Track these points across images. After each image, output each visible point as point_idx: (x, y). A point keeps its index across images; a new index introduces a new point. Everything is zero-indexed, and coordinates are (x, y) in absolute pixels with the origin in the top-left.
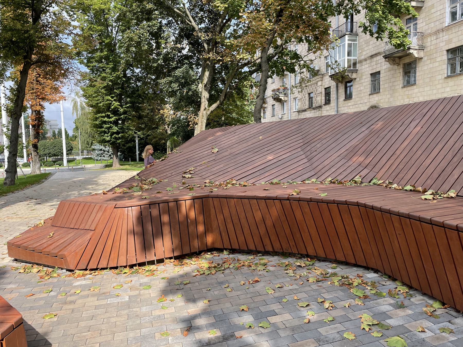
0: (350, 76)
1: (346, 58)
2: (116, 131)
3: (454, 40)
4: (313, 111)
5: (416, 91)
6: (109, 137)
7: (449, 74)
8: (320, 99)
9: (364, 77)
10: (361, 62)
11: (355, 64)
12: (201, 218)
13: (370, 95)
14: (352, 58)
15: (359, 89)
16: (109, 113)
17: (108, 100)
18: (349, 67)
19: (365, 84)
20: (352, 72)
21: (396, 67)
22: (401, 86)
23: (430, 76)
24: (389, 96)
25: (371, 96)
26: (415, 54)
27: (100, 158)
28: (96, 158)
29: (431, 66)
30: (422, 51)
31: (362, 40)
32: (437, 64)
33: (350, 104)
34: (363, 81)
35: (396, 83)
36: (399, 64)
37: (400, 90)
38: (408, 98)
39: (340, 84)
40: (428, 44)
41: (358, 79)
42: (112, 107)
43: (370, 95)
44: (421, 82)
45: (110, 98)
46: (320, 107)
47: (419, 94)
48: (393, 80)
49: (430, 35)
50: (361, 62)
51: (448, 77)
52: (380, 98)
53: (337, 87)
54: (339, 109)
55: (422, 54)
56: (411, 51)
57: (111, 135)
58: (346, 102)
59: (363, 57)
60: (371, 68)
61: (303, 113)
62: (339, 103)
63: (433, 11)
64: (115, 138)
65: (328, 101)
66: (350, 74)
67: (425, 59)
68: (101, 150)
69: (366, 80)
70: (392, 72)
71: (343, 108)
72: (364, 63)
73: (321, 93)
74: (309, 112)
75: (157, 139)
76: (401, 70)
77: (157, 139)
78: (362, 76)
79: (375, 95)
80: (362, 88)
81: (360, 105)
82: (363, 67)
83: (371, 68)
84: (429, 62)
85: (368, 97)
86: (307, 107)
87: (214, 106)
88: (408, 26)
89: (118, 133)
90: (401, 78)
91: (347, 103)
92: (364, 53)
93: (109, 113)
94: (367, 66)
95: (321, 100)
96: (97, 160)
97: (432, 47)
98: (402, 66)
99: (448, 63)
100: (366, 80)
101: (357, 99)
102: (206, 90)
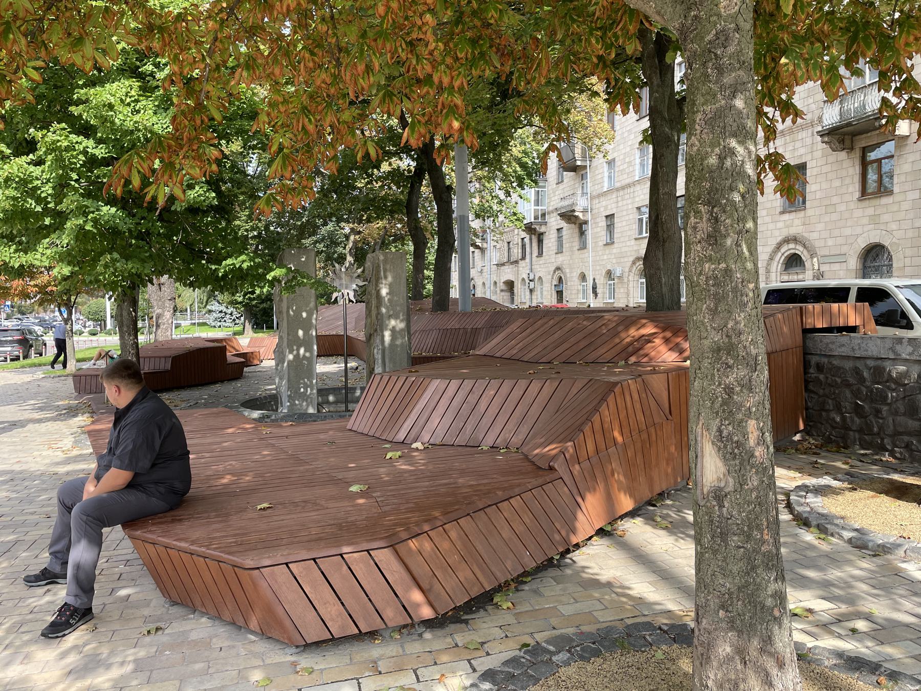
1: (533, 207)
3: (609, 207)
4: (511, 266)
6: (242, 297)
7: (608, 241)
8: (516, 252)
9: (552, 232)
10: (549, 213)
11: (543, 215)
14: (540, 208)
18: (536, 218)
20: (541, 224)
22: (577, 248)
24: (569, 258)
25: (557, 256)
26: (580, 215)
27: (219, 324)
28: (213, 324)
31: (550, 188)
32: (599, 229)
33: (541, 262)
36: (575, 224)
39: (533, 236)
41: (547, 234)
46: (516, 262)
50: (549, 213)
51: (607, 244)
52: (563, 258)
53: (531, 239)
56: (576, 214)
57: (244, 296)
58: (539, 259)
59: (551, 208)
61: (502, 268)
65: (523, 258)
66: (537, 227)
68: (221, 312)
72: (552, 215)
73: (518, 244)
74: (507, 267)
76: (577, 230)
81: (549, 265)
86: (505, 260)
90: (577, 239)
92: (552, 203)
95: (518, 252)
96: (215, 327)
101: (547, 257)
102: (350, 255)
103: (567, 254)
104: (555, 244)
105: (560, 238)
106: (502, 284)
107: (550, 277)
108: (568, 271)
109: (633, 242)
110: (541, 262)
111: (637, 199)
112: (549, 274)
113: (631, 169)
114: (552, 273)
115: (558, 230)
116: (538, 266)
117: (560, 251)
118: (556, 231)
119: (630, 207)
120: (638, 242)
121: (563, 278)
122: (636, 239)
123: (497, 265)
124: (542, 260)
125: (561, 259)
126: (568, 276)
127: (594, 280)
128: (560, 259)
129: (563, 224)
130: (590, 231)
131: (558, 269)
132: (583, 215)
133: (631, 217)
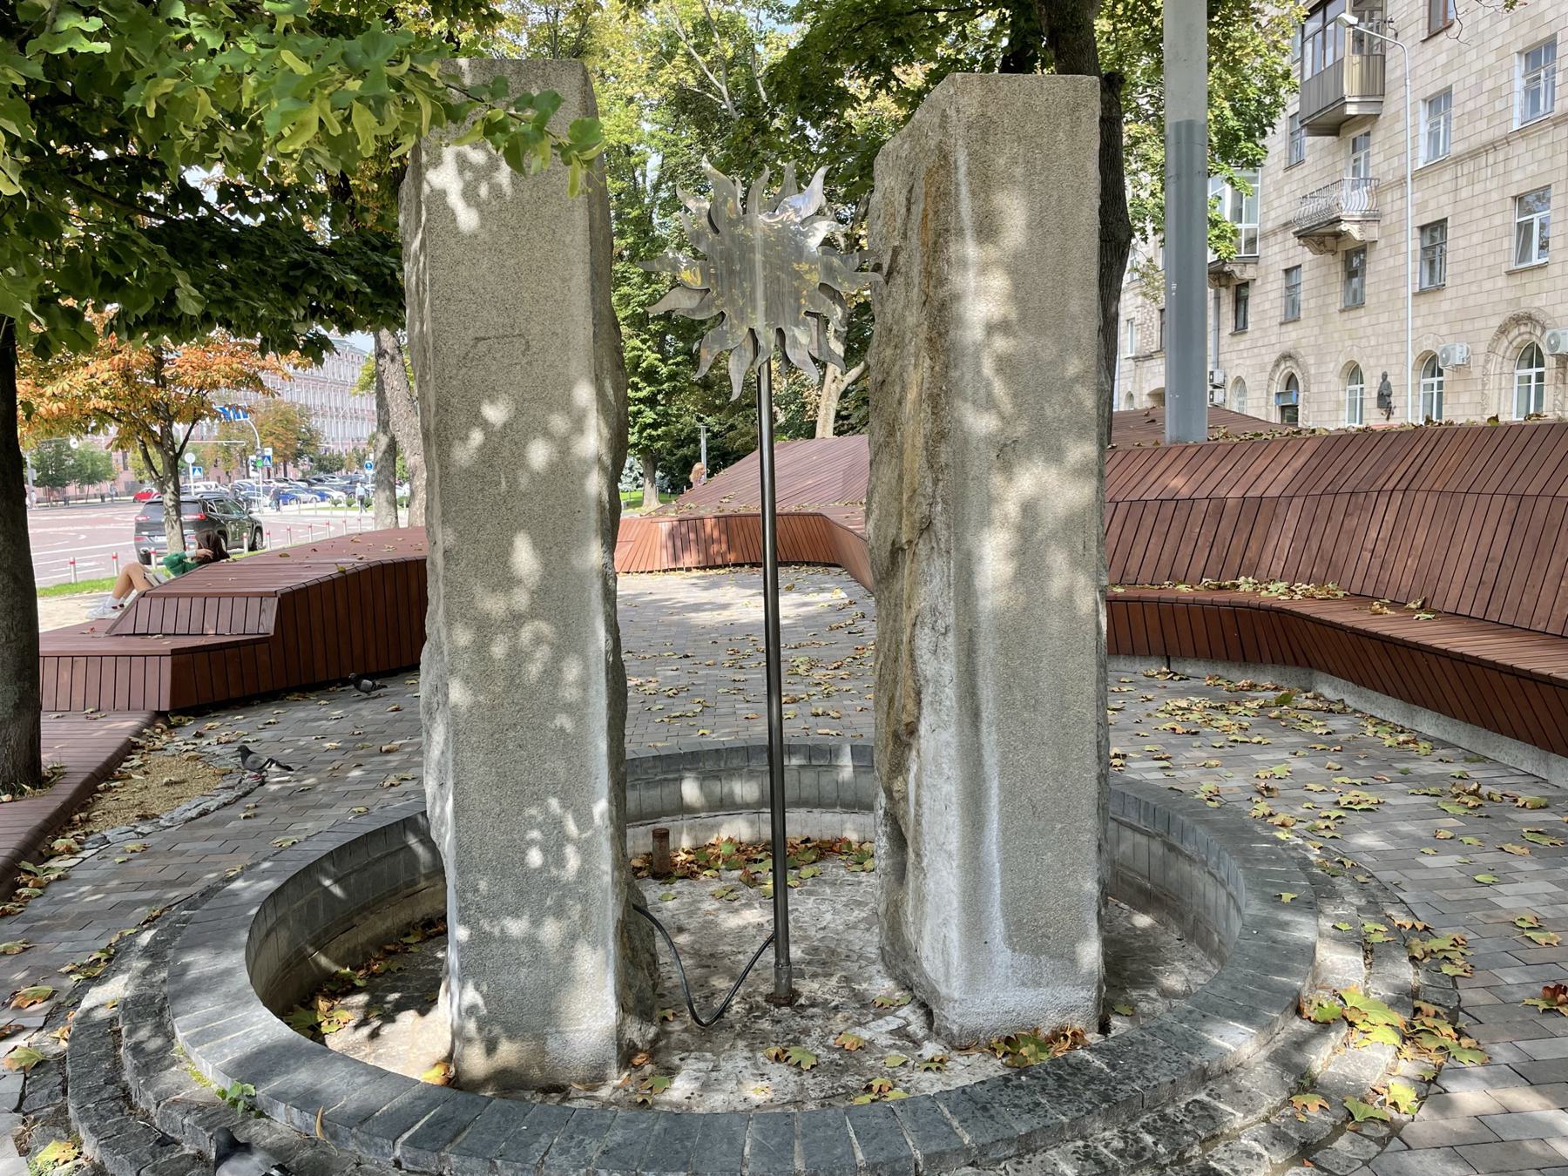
0: (1238, 273)
2: (651, 421)
3: (1432, 204)
5: (1365, 321)
6: (636, 436)
7: (1426, 285)
9: (1271, 278)
10: (1265, 236)
11: (1251, 242)
12: (724, 538)
13: (1282, 324)
15: (1260, 309)
16: (636, 379)
17: (634, 349)
19: (1272, 296)
20: (1244, 262)
21: (1329, 257)
22: (1338, 306)
23: (1388, 287)
24: (1316, 331)
25: (1284, 328)
26: (1354, 231)
29: (1391, 262)
30: (1376, 224)
31: (1268, 181)
33: (1242, 346)
34: (1269, 287)
35: (1329, 300)
36: (1334, 253)
37: (1337, 316)
38: (1351, 338)
39: (1223, 291)
40: (1387, 208)
41: (1258, 282)
42: (644, 365)
43: (1282, 324)
44: (1374, 300)
45: (637, 343)
47: (1369, 331)
48: (1324, 290)
49: (1391, 186)
50: (1265, 236)
51: (1422, 292)
54: (1222, 358)
55: (1373, 232)
56: (1344, 227)
57: (641, 432)
58: (1236, 339)
59: (1269, 226)
60: (1283, 255)
61: (1147, 364)
62: (1222, 342)
63: (1399, 127)
64: (650, 437)
66: (1237, 270)
67: (1382, 243)
69: (1275, 286)
70: (1324, 269)
71: (1228, 356)
72: (1272, 240)
75: (748, 438)
76: (1340, 267)
77: (748, 438)
78: (1267, 274)
79: (1290, 327)
80: (1267, 306)
81: (1263, 351)
82: (1270, 251)
83: (1283, 255)
84: (1386, 253)
85: (1276, 329)
87: (855, 372)
88: (1356, 156)
89: (655, 426)
90: (1338, 287)
91: (1238, 343)
92: (1273, 214)
93: (636, 379)
94: (1276, 249)
97: (1395, 217)
98: (1340, 256)
99: (1422, 259)
100: (1275, 286)
101: (1258, 334)
103: (1312, 322)
104: (1280, 302)
105: (1291, 288)
106: (1144, 398)
107: (1266, 376)
108: (1311, 360)
109: (1501, 282)
110: (1242, 346)
111: (1517, 176)
112: (1263, 370)
113: (1499, 105)
114: (1269, 368)
115: (1287, 271)
116: (1234, 355)
117: (1292, 314)
118: (1281, 275)
119: (1495, 196)
120: (1517, 280)
121: (1298, 376)
122: (1510, 273)
123: (1136, 359)
124: (1244, 342)
125: (1294, 335)
126: (1312, 371)
127: (1385, 376)
128: (1292, 336)
129: (1306, 256)
130: (1377, 267)
131: (1287, 357)
132: (1362, 230)
133: (1497, 220)
